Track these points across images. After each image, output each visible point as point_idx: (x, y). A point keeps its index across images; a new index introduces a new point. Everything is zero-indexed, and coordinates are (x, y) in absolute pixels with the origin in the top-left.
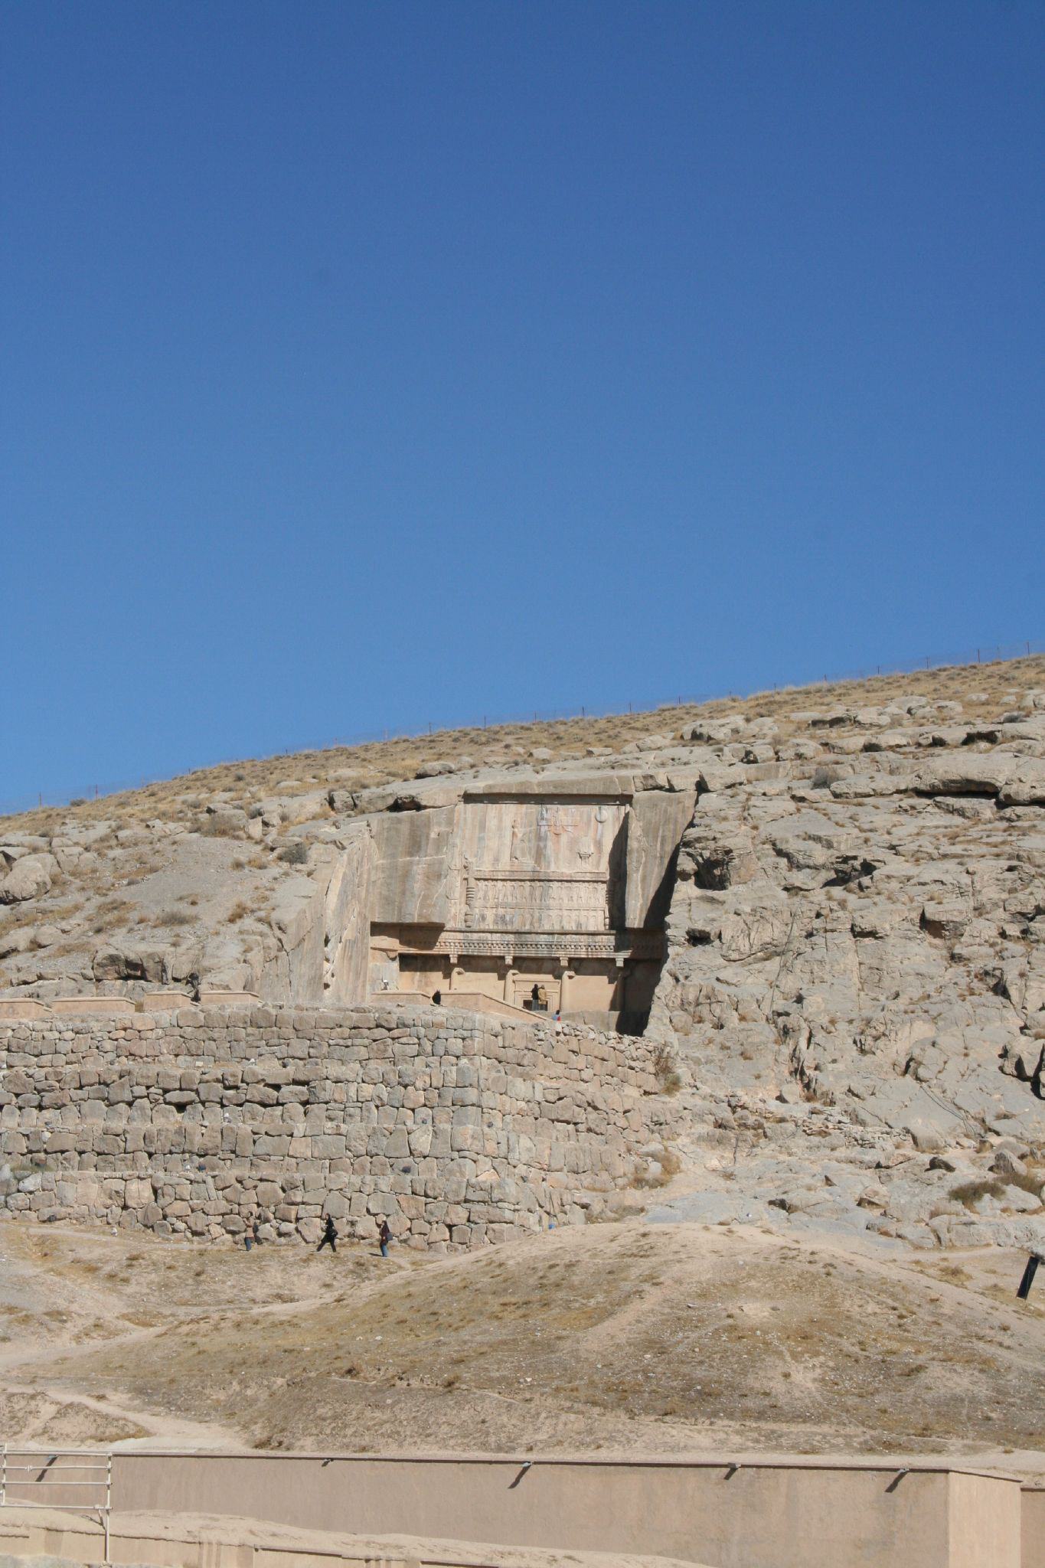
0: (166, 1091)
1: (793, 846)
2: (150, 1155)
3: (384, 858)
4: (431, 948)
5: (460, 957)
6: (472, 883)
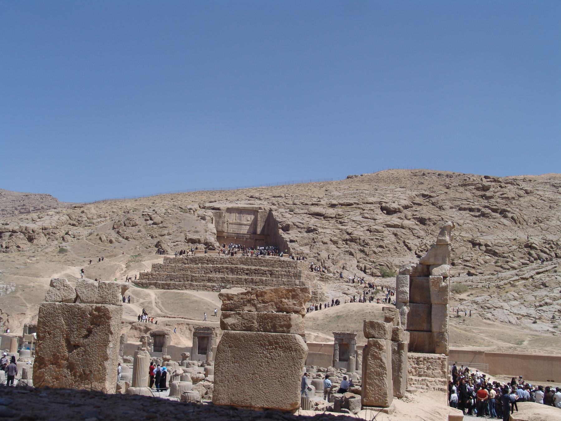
1: (297, 224)
2: (246, 282)
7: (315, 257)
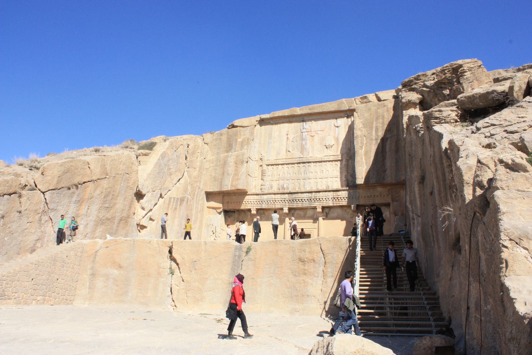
3: (213, 155)
5: (258, 210)
6: (265, 167)
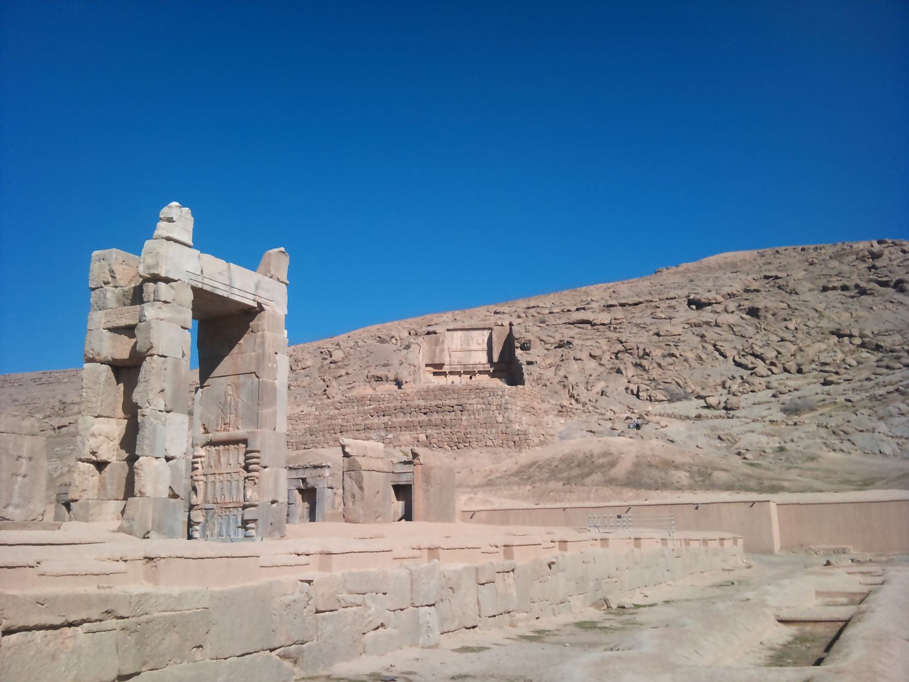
0: (420, 409)
1: (544, 338)
2: (421, 427)
4: (442, 369)
5: (449, 372)
6: (451, 352)
7: (561, 382)
